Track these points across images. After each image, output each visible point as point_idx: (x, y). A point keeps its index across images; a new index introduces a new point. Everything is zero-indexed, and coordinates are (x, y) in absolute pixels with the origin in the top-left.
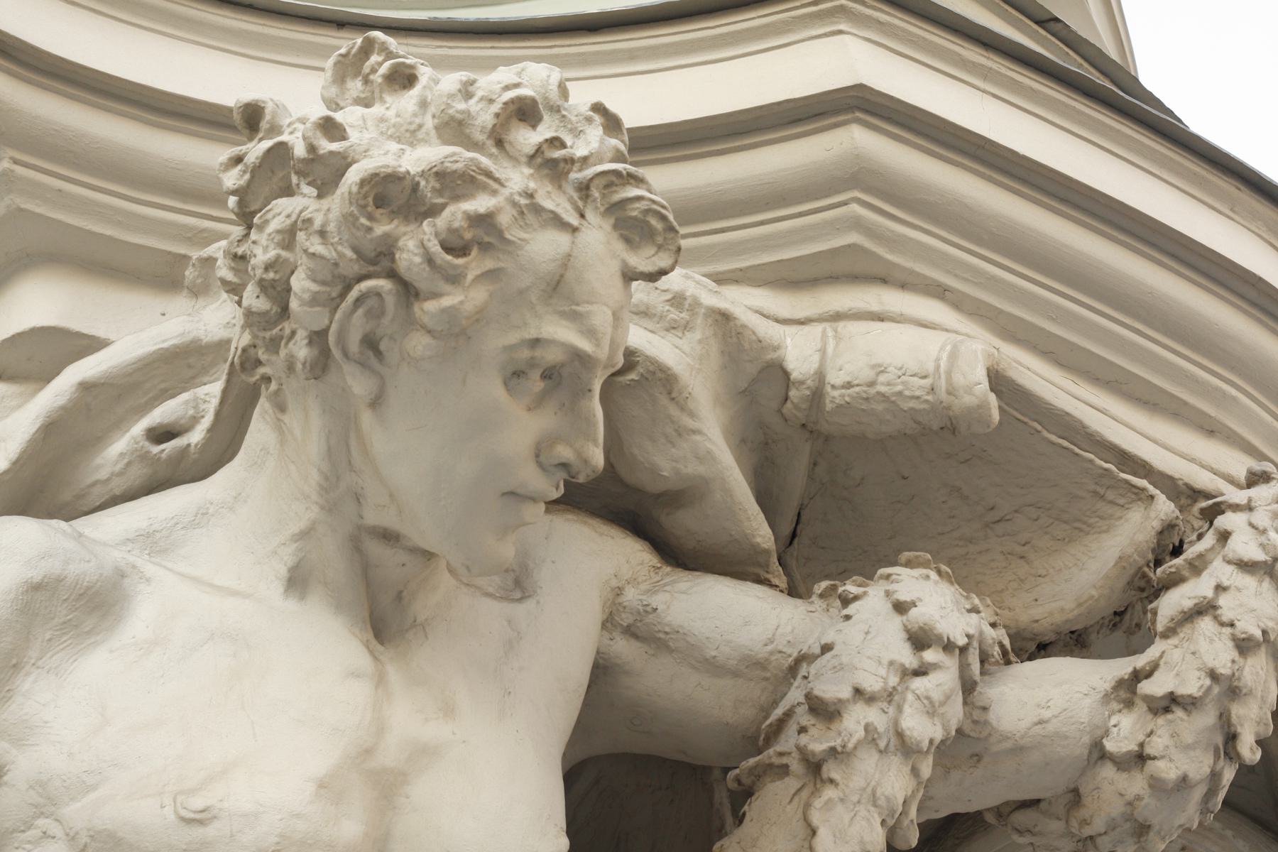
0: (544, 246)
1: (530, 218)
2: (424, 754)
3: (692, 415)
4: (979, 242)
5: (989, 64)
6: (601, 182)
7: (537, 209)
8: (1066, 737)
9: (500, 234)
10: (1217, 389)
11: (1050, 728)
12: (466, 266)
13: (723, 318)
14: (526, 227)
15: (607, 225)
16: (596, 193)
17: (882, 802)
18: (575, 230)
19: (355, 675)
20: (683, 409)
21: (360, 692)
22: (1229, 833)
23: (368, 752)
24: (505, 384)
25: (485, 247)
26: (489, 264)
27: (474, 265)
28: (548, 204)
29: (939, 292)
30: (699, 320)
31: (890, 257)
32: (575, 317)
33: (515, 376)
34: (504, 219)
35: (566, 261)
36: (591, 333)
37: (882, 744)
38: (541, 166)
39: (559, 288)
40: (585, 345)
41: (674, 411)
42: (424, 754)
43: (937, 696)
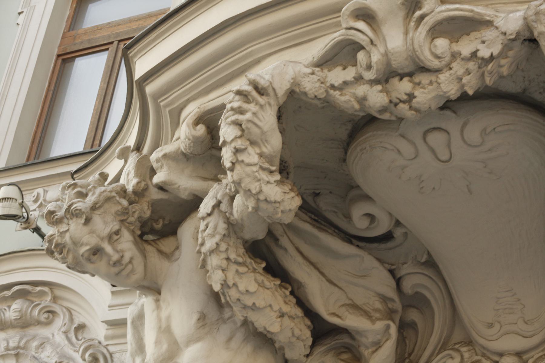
0: (67, 238)
1: (63, 235)
2: (169, 318)
3: (176, 184)
4: (178, 85)
5: (155, 35)
6: (67, 213)
7: (61, 233)
8: (243, 211)
9: (60, 244)
10: (246, 54)
11: (239, 211)
12: (64, 255)
13: (165, 156)
14: (64, 237)
15: (74, 219)
16: (68, 216)
17: (216, 268)
18: (68, 230)
19: (153, 311)
20: (173, 185)
21: (155, 313)
22: (375, 132)
23: (160, 328)
24: (92, 263)
25: (64, 247)
26: (67, 250)
27: (65, 252)
28: (61, 230)
29: (188, 101)
30: (163, 161)
31: (175, 106)
32: (82, 245)
33: (89, 260)
34: (59, 241)
35: (71, 238)
36: (87, 244)
37: (208, 254)
38: (56, 224)
39: (76, 243)
40: (88, 247)
41: (173, 187)
42: (169, 318)
43: (210, 232)
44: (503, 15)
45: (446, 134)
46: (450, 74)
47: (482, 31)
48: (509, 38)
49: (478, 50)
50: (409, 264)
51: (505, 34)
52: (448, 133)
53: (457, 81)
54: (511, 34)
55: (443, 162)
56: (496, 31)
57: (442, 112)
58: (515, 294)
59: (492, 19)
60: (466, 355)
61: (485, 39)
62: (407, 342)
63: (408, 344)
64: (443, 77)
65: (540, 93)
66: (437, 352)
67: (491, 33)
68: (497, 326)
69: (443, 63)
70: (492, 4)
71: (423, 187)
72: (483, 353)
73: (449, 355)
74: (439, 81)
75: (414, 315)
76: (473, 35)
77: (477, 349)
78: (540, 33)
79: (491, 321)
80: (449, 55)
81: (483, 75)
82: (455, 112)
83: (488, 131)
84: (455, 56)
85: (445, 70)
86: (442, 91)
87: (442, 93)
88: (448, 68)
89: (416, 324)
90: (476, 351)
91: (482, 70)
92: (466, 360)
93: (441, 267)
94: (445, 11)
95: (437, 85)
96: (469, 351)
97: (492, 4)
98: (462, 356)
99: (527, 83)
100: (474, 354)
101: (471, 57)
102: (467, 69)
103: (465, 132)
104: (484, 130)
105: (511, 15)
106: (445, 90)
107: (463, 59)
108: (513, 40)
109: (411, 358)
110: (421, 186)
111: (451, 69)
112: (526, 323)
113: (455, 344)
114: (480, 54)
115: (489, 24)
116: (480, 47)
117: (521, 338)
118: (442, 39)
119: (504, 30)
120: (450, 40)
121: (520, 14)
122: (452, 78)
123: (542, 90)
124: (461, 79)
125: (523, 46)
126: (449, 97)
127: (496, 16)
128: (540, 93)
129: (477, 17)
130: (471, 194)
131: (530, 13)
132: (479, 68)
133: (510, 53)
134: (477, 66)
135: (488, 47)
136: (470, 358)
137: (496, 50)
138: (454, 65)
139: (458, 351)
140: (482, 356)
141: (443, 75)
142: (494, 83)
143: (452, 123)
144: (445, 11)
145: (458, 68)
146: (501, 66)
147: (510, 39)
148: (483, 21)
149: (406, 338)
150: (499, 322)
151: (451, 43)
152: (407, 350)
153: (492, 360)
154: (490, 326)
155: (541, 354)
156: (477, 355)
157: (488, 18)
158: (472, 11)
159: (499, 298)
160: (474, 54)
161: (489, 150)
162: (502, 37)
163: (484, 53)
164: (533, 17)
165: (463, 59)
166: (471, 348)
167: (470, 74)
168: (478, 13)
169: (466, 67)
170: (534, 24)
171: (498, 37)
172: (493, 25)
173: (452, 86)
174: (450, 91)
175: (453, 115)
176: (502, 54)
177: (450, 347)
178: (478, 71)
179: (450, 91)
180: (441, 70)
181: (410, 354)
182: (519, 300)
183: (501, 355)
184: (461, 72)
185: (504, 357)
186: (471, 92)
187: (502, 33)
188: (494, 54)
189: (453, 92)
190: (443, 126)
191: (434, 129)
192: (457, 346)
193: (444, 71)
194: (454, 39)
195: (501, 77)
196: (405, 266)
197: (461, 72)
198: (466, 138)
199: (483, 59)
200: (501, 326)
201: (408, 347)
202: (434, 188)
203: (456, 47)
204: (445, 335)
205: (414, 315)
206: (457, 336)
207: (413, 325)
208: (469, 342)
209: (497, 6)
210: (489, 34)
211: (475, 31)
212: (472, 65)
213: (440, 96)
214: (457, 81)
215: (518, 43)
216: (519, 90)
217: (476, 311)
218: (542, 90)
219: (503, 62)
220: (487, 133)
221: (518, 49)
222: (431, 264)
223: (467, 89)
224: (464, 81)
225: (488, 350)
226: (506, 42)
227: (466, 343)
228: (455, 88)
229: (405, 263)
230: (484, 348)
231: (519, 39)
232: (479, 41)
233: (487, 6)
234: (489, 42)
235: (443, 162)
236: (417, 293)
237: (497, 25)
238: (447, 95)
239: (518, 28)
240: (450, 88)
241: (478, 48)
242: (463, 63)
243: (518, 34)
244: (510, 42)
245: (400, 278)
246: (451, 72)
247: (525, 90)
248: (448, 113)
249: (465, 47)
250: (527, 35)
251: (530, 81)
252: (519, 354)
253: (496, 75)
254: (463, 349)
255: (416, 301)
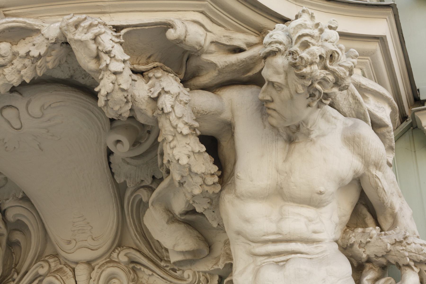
44: (47, 25)
45: (16, 110)
46: (12, 68)
47: (33, 37)
48: (50, 42)
49: (30, 51)
50: (10, 200)
51: (48, 39)
52: (18, 109)
53: (18, 73)
54: (52, 40)
55: (16, 129)
56: (42, 37)
57: (11, 95)
58: (85, 219)
59: (39, 28)
60: (53, 265)
61: (35, 42)
62: (14, 256)
63: (14, 257)
64: (7, 70)
65: (83, 78)
66: (34, 262)
67: (39, 38)
68: (74, 242)
69: (7, 60)
70: (41, 17)
71: (6, 147)
72: (66, 262)
73: (41, 265)
74: (5, 73)
75: (17, 236)
76: (28, 39)
77: (61, 260)
78: (70, 39)
79: (70, 240)
80: (11, 55)
81: (35, 68)
82: (21, 94)
83: (46, 107)
84: (15, 55)
85: (9, 65)
86: (7, 81)
87: (7, 82)
88: (11, 64)
89: (20, 243)
90: (60, 261)
91: (34, 65)
92: (52, 268)
93: (32, 201)
94: (5, 23)
95: (4, 76)
96: (55, 261)
97: (41, 17)
98: (50, 266)
99: (72, 72)
100: (59, 263)
101: (27, 55)
102: (24, 64)
103: (29, 108)
104: (43, 106)
105: (52, 25)
106: (9, 80)
107: (20, 57)
108: (54, 43)
109: (17, 268)
110: (5, 146)
111: (13, 64)
112: (93, 240)
113: (46, 256)
114: (31, 54)
115: (38, 31)
116: (32, 48)
117: (90, 250)
118: (5, 43)
119: (47, 36)
120: (11, 43)
121: (58, 25)
122: (13, 71)
123: (83, 76)
124: (20, 71)
125: (62, 47)
126: (12, 84)
127: (42, 26)
128: (83, 78)
129: (29, 26)
130: (42, 150)
131: (64, 24)
132: (32, 63)
133: (53, 53)
134: (30, 62)
135: (37, 48)
136: (55, 266)
137: (43, 50)
138: (15, 61)
139: (47, 262)
140: (64, 265)
141: (7, 69)
142: (43, 75)
143: (19, 101)
144: (5, 23)
145: (18, 64)
146: (47, 62)
147: (51, 43)
148: (34, 30)
149: (14, 253)
150: (75, 240)
151: (13, 45)
152: (14, 262)
153: (71, 267)
154: (69, 242)
155: (104, 262)
156: (61, 264)
157: (37, 28)
158: (25, 23)
159: (74, 223)
160: (28, 53)
161: (49, 120)
162: (46, 41)
163: (35, 53)
164: (65, 28)
165: (20, 57)
166: (57, 259)
167: (26, 68)
168: (30, 24)
169: (23, 63)
170: (66, 32)
171: (44, 41)
172: (40, 32)
173: (14, 77)
174: (12, 81)
175: (20, 96)
176: (47, 54)
177: (43, 259)
178: (32, 66)
179: (12, 81)
180: (6, 65)
181: (16, 265)
182: (88, 223)
183: (77, 263)
184: (19, 66)
185: (78, 265)
186: (28, 81)
187: (46, 38)
188: (41, 54)
189: (15, 81)
190: (13, 104)
191: (8, 106)
192: (46, 258)
193: (8, 66)
194: (14, 42)
195: (48, 69)
196: (8, 201)
197: (19, 66)
198: (30, 112)
199: (33, 57)
200: (76, 243)
201: (14, 260)
202: (15, 148)
203: (15, 49)
204: (39, 250)
205: (17, 236)
206: (49, 251)
207: (18, 243)
208: (56, 255)
209: (44, 18)
210: (38, 39)
211: (29, 37)
212: (27, 62)
213: (6, 84)
214: (18, 73)
215: (58, 46)
216: (67, 77)
217: (59, 233)
218: (83, 76)
219: (48, 59)
220: (45, 108)
221: (58, 50)
222: (25, 199)
223: (24, 78)
224: (22, 73)
225: (68, 261)
226: (49, 45)
227: (54, 255)
228: (17, 78)
229: (8, 199)
230: (66, 259)
231: (59, 42)
232: (31, 44)
233: (37, 18)
234: (37, 45)
235: (16, 129)
236: (18, 220)
237: (42, 33)
238: (11, 83)
239: (56, 35)
240: (13, 78)
241: (30, 49)
242: (21, 60)
243: (57, 39)
244: (52, 45)
245: (5, 210)
246: (13, 66)
247: (72, 76)
248: (16, 95)
249: (22, 48)
250: (63, 40)
251: (74, 70)
252: (89, 263)
253: (45, 68)
254: (51, 260)
255: (20, 226)
